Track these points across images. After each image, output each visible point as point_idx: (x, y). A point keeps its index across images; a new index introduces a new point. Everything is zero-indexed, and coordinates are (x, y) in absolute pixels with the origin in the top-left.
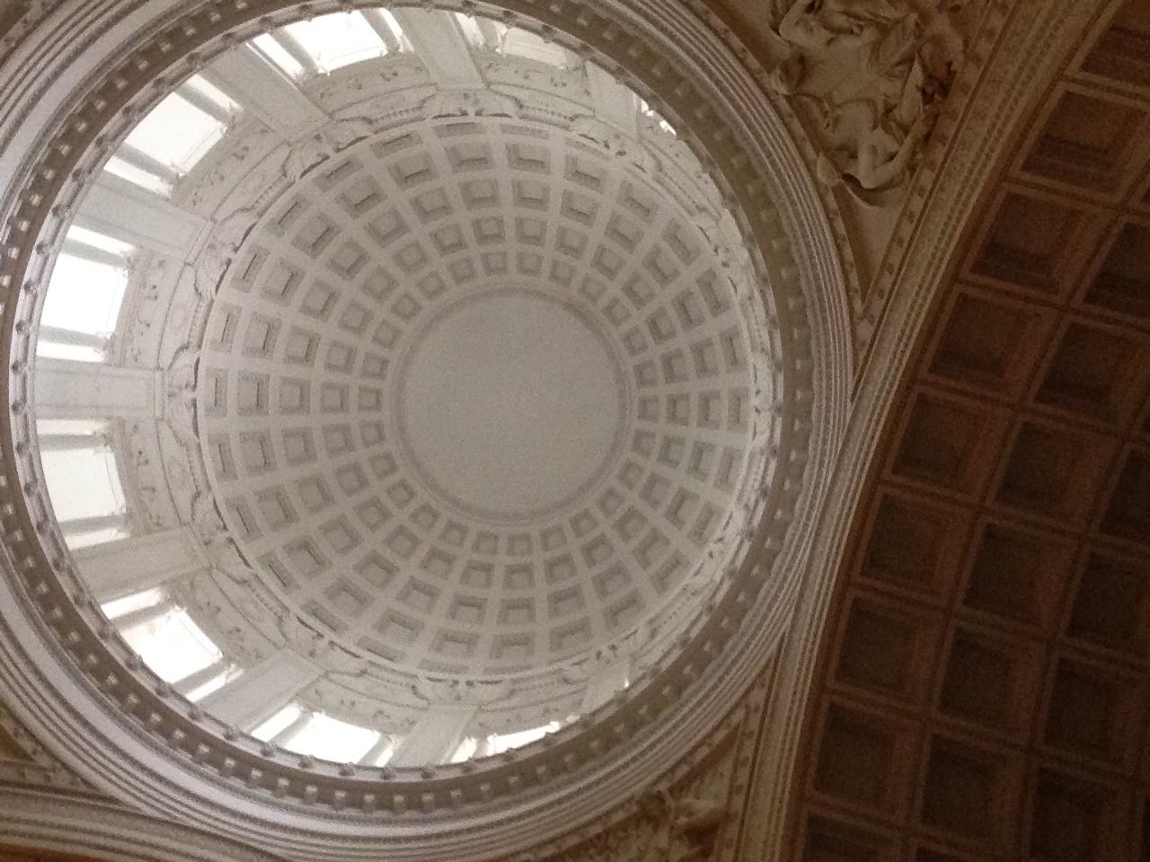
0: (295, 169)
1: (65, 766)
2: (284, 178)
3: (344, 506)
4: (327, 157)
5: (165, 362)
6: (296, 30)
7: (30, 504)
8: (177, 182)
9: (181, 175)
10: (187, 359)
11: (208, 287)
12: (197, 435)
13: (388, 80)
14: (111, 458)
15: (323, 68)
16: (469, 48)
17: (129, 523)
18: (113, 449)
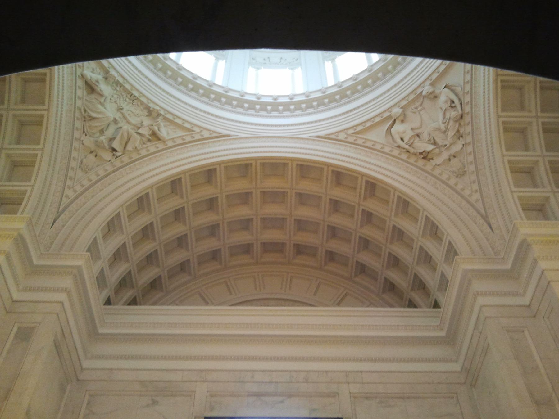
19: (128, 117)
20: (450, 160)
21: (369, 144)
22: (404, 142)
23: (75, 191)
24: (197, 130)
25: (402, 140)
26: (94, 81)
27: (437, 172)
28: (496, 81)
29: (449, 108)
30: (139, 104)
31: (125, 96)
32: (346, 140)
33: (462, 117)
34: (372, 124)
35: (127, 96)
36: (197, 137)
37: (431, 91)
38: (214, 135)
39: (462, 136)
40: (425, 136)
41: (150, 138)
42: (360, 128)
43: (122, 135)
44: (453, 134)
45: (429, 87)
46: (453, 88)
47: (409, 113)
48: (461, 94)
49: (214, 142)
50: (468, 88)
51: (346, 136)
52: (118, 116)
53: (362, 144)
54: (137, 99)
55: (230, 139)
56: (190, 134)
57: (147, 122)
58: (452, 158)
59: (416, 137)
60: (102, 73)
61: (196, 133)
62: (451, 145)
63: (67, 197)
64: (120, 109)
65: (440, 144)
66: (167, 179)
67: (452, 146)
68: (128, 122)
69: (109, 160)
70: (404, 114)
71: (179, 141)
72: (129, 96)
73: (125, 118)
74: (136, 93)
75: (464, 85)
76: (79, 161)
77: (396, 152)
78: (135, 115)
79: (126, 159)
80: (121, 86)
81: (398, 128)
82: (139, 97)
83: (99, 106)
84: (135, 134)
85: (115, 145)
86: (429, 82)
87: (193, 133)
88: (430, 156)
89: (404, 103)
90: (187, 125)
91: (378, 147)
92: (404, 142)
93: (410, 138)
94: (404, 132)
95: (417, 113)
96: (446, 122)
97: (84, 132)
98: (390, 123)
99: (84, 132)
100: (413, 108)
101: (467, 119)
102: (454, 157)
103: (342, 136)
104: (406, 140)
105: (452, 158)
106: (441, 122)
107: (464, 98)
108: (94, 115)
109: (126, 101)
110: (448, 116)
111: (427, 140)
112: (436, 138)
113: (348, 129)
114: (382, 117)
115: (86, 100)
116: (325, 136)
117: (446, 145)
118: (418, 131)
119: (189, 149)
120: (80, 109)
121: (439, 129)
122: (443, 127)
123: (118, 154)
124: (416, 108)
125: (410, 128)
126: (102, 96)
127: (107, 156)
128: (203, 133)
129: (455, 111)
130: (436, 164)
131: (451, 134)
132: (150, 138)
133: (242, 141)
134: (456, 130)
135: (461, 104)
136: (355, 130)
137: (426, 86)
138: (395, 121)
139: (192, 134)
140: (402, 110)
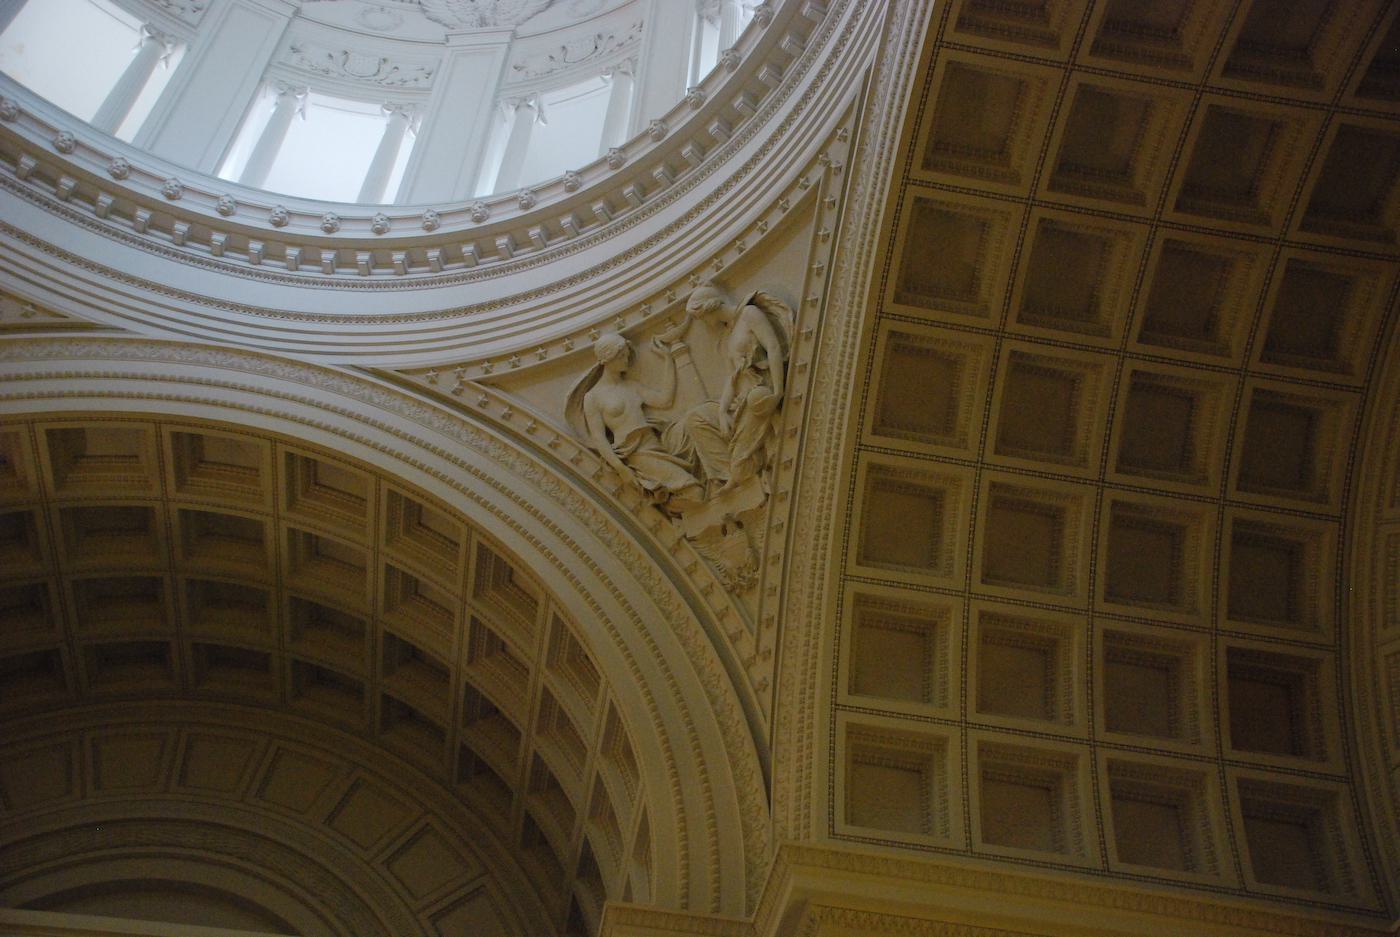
1: (822, 149)
5: (440, 32)
8: (157, 37)
9: (147, 35)
20: (724, 531)
21: (519, 425)
25: (609, 434)
27: (687, 557)
28: (872, 334)
29: (746, 371)
32: (455, 398)
33: (780, 406)
38: (40, 319)
39: (769, 468)
40: (675, 439)
42: (502, 369)
44: (745, 455)
45: (712, 290)
46: (773, 309)
47: (646, 351)
48: (789, 333)
49: (32, 341)
50: (811, 321)
51: (456, 385)
53: (500, 421)
58: (730, 527)
59: (651, 435)
62: (736, 485)
65: (709, 476)
67: (739, 489)
81: (606, 395)
86: (710, 274)
88: (675, 504)
89: (634, 321)
91: (542, 440)
92: (612, 442)
93: (630, 437)
94: (618, 413)
95: (667, 362)
96: (736, 414)
100: (658, 342)
101: (795, 416)
102: (739, 525)
103: (446, 385)
104: (619, 440)
105: (730, 527)
106: (722, 408)
107: (796, 348)
110: (742, 395)
112: (699, 454)
113: (466, 365)
114: (568, 349)
117: (724, 482)
118: (657, 416)
121: (714, 428)
122: (724, 421)
124: (667, 344)
125: (638, 403)
129: (763, 384)
131: (741, 453)
133: (130, 349)
134: (754, 445)
135: (786, 365)
136: (487, 372)
137: (701, 284)
138: (600, 369)
140: (622, 341)
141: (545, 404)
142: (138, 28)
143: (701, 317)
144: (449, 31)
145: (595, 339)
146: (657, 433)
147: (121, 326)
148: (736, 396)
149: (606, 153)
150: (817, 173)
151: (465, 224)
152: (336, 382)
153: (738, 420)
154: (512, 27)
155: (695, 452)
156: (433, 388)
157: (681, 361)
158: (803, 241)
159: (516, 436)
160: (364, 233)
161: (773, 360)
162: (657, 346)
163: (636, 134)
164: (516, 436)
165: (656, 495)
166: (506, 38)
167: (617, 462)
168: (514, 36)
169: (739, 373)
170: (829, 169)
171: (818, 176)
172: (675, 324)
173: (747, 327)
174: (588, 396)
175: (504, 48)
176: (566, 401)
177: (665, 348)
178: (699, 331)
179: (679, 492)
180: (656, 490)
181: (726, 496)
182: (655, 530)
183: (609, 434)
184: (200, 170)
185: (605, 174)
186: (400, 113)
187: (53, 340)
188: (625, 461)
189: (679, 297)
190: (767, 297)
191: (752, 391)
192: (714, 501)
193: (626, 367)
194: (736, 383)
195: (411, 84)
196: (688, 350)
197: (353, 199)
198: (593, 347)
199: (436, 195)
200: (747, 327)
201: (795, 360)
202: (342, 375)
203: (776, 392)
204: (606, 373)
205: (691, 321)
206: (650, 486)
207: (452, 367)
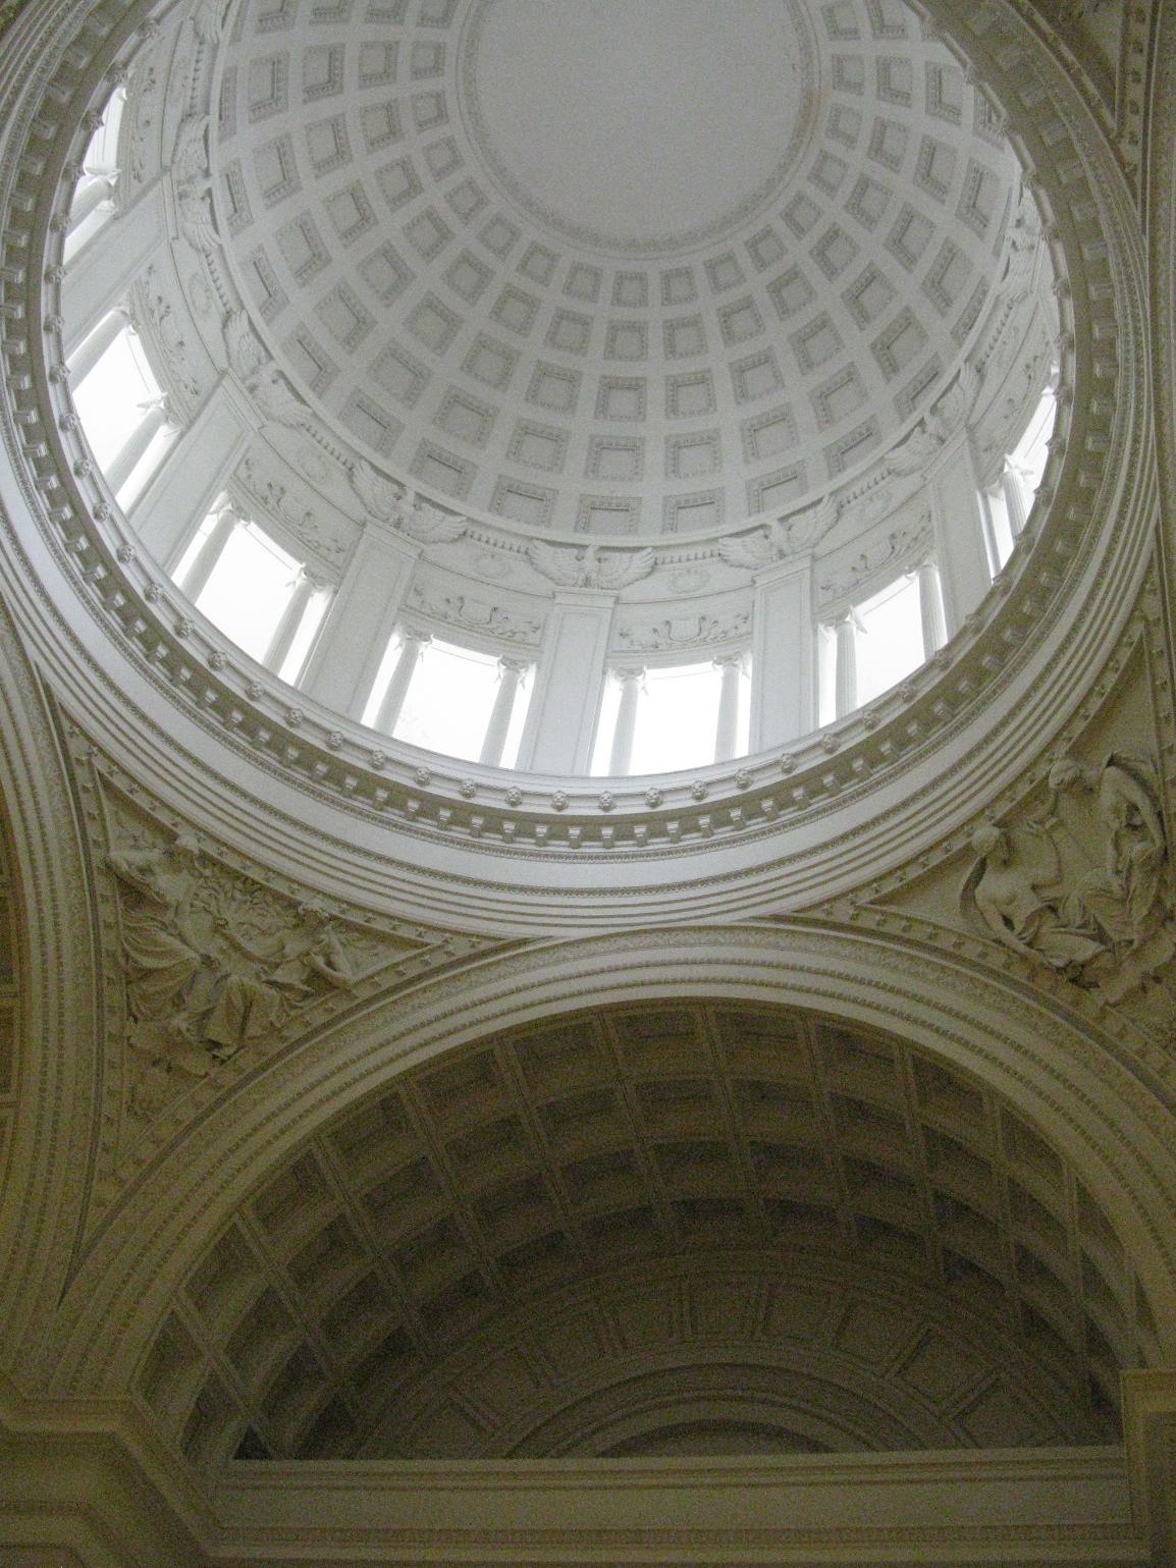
0: (451, 526)
2: (469, 533)
3: (777, 335)
4: (419, 496)
5: (745, 575)
6: (257, 647)
7: (925, 689)
8: (513, 665)
10: (736, 549)
11: (640, 562)
12: (820, 501)
13: (282, 490)
14: (860, 610)
15: (299, 575)
16: (182, 436)
17: (925, 563)
18: (847, 612)
19: (244, 943)
20: (1144, 989)
22: (1012, 929)
23: (121, 1182)
24: (434, 939)
25: (1008, 922)
26: (135, 874)
29: (1124, 832)
30: (269, 899)
31: (228, 886)
34: (921, 871)
35: (234, 887)
36: (439, 959)
37: (1068, 776)
38: (484, 945)
40: (1072, 913)
41: (308, 989)
42: (891, 886)
43: (229, 1002)
44: (1145, 911)
45: (1068, 762)
47: (1020, 834)
51: (851, 912)
52: (215, 947)
54: (262, 888)
55: (527, 954)
56: (415, 957)
57: (295, 946)
58: (1150, 983)
59: (1048, 913)
60: (160, 842)
61: (432, 951)
62: (1144, 942)
63: (101, 1203)
64: (219, 928)
65: (1116, 937)
66: (370, 1095)
68: (248, 956)
69: (203, 1073)
70: (1008, 842)
71: (390, 981)
72: (239, 885)
73: (237, 947)
74: (255, 874)
75: (1161, 757)
76: (126, 1096)
77: (997, 960)
78: (263, 933)
79: (248, 1061)
80: (214, 863)
81: (996, 885)
82: (264, 883)
83: (163, 936)
84: (265, 989)
85: (215, 1031)
86: (1063, 748)
87: (424, 949)
89: (1002, 810)
90: (407, 933)
91: (946, 942)
92: (1012, 929)
93: (1030, 920)
94: (1010, 901)
97: (130, 1013)
98: (971, 869)
99: (130, 1013)
100: (1031, 823)
102: (1157, 980)
103: (843, 912)
104: (1019, 927)
106: (1109, 872)
108: (148, 962)
109: (233, 898)
111: (1079, 922)
112: (1099, 920)
115: (129, 928)
116: (795, 915)
117: (1131, 942)
119: (416, 1001)
120: (112, 955)
121: (1105, 892)
122: (1116, 884)
123: (223, 1053)
124: (1041, 822)
126: (166, 906)
127: (197, 1064)
128: (451, 948)
130: (1107, 1003)
131: (1140, 910)
132: (308, 989)
133: (563, 953)
134: (1151, 900)
135: (1160, 815)
138: (983, 865)
139: (422, 955)
140: (996, 832)
141: (938, 909)
142: (495, 664)
143: (1065, 791)
144: (754, 573)
145: (969, 835)
146: (1053, 910)
147: (546, 934)
148: (1120, 855)
149: (932, 654)
150: (1138, 629)
151: (820, 758)
152: (743, 937)
153: (1128, 879)
154: (810, 551)
155: (1096, 921)
156: (831, 918)
157: (1057, 836)
158: (1142, 695)
159: (920, 945)
160: (731, 792)
161: (1146, 814)
162: (1031, 827)
163: (955, 633)
164: (920, 945)
165: (1069, 970)
166: (807, 563)
167: (1022, 948)
168: (814, 558)
169: (1117, 834)
170: (1147, 624)
171: (1139, 633)
172: (1043, 803)
173: (1113, 789)
174: (979, 892)
175: (808, 573)
176: (958, 902)
177: (1039, 827)
178: (1067, 804)
179: (1091, 961)
180: (1067, 965)
181: (1136, 955)
182: (1076, 1003)
183: (1008, 922)
184: (576, 774)
185: (937, 677)
186: (728, 661)
187: (498, 962)
188: (1029, 945)
189: (1039, 778)
190: (1124, 755)
191: (1136, 849)
192: (1125, 964)
193: (1007, 854)
194: (1117, 845)
195: (732, 633)
196: (1061, 823)
197: (710, 760)
198: (970, 843)
199: (784, 736)
200: (1113, 789)
201: (1167, 809)
202: (746, 929)
203: (1158, 843)
204: (989, 868)
205: (1057, 796)
206: (1059, 963)
207: (843, 895)
